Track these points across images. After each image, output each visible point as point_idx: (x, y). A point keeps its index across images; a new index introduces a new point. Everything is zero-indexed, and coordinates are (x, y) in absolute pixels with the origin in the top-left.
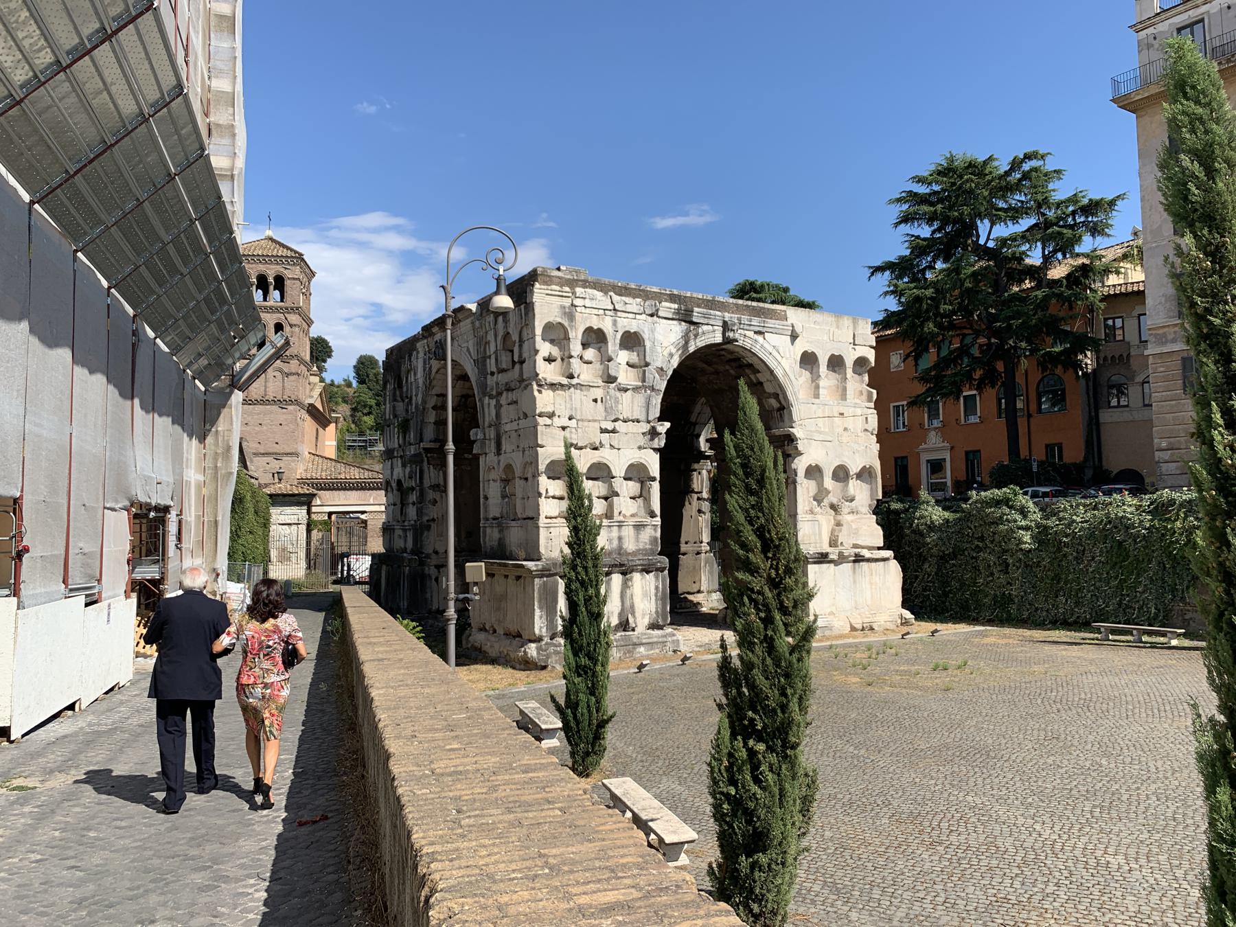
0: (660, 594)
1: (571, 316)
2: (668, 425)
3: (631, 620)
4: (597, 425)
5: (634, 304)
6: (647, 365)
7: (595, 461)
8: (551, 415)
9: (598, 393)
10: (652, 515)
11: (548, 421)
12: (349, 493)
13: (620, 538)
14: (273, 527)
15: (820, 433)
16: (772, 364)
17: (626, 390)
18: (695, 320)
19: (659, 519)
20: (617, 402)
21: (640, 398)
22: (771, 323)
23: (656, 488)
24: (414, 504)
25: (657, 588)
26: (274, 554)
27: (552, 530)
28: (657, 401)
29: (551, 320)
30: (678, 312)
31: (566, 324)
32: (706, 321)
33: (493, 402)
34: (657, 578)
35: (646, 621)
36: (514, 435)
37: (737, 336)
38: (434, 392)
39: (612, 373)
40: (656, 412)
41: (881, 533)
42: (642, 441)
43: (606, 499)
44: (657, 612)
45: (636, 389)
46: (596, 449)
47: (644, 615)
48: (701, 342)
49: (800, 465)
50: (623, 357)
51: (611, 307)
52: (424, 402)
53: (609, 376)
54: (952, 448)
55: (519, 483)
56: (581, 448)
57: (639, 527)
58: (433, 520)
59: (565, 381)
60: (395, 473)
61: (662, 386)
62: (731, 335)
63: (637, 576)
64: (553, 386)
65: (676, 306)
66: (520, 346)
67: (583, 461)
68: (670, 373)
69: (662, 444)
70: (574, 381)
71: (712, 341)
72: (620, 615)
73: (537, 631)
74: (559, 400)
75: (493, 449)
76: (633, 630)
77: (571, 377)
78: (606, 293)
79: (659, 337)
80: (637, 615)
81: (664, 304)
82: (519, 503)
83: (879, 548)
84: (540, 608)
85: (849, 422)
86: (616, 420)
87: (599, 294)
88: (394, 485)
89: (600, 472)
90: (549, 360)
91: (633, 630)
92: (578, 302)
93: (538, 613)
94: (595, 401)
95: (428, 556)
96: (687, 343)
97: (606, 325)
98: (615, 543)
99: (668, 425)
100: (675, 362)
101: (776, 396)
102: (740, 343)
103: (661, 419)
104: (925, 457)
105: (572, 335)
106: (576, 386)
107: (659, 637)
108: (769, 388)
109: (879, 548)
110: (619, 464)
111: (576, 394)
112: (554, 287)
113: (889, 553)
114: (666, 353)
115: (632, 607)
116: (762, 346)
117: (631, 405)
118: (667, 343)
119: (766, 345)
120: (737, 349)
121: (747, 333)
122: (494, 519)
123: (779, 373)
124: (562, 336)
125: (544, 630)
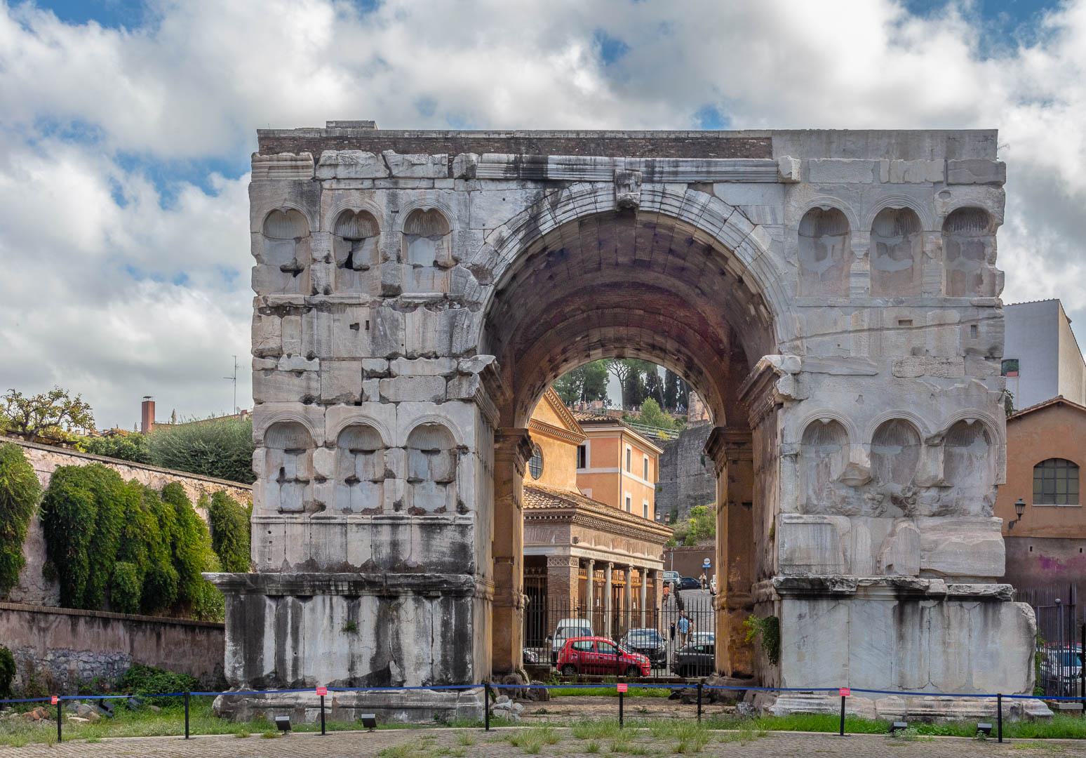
3: (394, 670)
4: (356, 365)
6: (457, 261)
7: (351, 422)
9: (362, 315)
10: (462, 509)
11: (269, 363)
13: (395, 545)
15: (844, 360)
17: (416, 306)
18: (552, 176)
20: (395, 325)
21: (438, 319)
22: (724, 164)
25: (445, 624)
27: (272, 528)
29: (278, 205)
30: (515, 166)
31: (303, 209)
32: (576, 176)
34: (446, 607)
35: (424, 674)
42: (439, 388)
45: (431, 304)
46: (358, 404)
47: (419, 665)
48: (566, 214)
51: (382, 173)
56: (329, 403)
57: (431, 528)
59: (299, 298)
61: (486, 294)
62: (622, 194)
63: (408, 605)
65: (512, 157)
68: (499, 271)
71: (591, 209)
72: (374, 661)
73: (228, 673)
74: (289, 330)
76: (400, 685)
80: (406, 664)
81: (485, 156)
83: (999, 580)
84: (234, 640)
85: (929, 340)
86: (389, 359)
87: (361, 155)
89: (359, 440)
92: (325, 173)
93: (229, 647)
94: (355, 327)
96: (535, 219)
97: (379, 203)
98: (385, 552)
100: (511, 251)
106: (321, 307)
107: (442, 700)
110: (393, 424)
112: (285, 155)
114: (491, 240)
115: (398, 649)
116: (704, 209)
119: (715, 206)
121: (670, 189)
125: (240, 673)
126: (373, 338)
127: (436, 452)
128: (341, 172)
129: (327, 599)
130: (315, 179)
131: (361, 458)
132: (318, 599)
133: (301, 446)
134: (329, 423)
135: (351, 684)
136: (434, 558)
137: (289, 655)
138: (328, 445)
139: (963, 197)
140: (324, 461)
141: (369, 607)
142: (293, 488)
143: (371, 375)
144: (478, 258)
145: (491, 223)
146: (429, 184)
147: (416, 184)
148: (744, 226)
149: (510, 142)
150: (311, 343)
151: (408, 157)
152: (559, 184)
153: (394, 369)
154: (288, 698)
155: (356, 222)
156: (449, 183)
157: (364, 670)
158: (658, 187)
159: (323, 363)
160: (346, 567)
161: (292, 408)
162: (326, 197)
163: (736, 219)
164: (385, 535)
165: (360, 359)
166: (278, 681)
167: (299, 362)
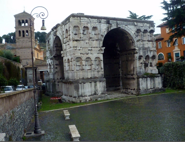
0: (104, 87)
1: (80, 24)
2: (104, 48)
3: (97, 92)
4: (87, 49)
5: (95, 20)
6: (99, 34)
7: (87, 57)
8: (76, 47)
9: (87, 41)
10: (102, 69)
11: (76, 48)
12: (44, 67)
14: (28, 75)
16: (130, 32)
18: (110, 23)
19: (103, 69)
21: (98, 42)
23: (102, 62)
24: (53, 68)
25: (103, 85)
26: (28, 81)
27: (77, 73)
28: (102, 42)
29: (75, 25)
32: (113, 23)
33: (65, 45)
34: (103, 83)
35: (101, 93)
36: (69, 52)
37: (120, 26)
38: (55, 43)
39: (91, 37)
40: (101, 45)
41: (158, 70)
42: (98, 52)
43: (91, 65)
44: (103, 91)
46: (87, 54)
47: (100, 91)
48: (112, 28)
49: (137, 56)
50: (93, 33)
52: (53, 46)
53: (90, 37)
54: (180, 50)
55: (71, 63)
57: (98, 72)
58: (57, 72)
59: (79, 39)
60: (49, 62)
61: (103, 39)
62: (119, 26)
64: (77, 41)
66: (69, 32)
67: (84, 57)
69: (103, 52)
70: (81, 39)
71: (114, 28)
72: (94, 92)
75: (66, 56)
77: (81, 38)
78: (88, 18)
79: (102, 28)
80: (98, 91)
81: (102, 20)
82: (71, 67)
86: (92, 47)
88: (49, 64)
90: (76, 34)
91: (98, 95)
92: (81, 21)
94: (87, 43)
95: (56, 80)
96: (108, 28)
99: (104, 48)
100: (106, 33)
101: (131, 40)
102: (121, 28)
103: (103, 47)
104: (174, 53)
105: (80, 28)
106: (82, 40)
108: (130, 38)
109: (157, 74)
110: (93, 57)
111: (82, 42)
112: (76, 18)
113: (159, 75)
114: (103, 31)
115: (97, 89)
116: (127, 28)
117: (95, 44)
118: (103, 29)
119: (128, 28)
120: (121, 29)
121: (123, 25)
122: (67, 71)
123: (132, 34)
124: (78, 29)
125: (77, 95)
126: (89, 45)
127: (96, 61)
128: (84, 21)
129: (88, 83)
130: (80, 22)
131: (87, 62)
132: (86, 83)
133: (79, 60)
134: (84, 57)
135: (91, 95)
136: (99, 76)
137: (83, 92)
138: (84, 60)
139: (152, 28)
140: (84, 63)
141: (93, 84)
142: (78, 67)
143: (90, 50)
144: (102, 34)
145: (103, 29)
146: (94, 23)
147: (93, 23)
148: (131, 31)
149: (104, 18)
150: (81, 45)
151: (92, 19)
152: (111, 24)
153: (92, 49)
154: (84, 98)
155: (86, 28)
156: (97, 23)
157: (93, 93)
158: (122, 25)
159: (83, 49)
160: (88, 78)
161: (79, 55)
162: (82, 24)
163: (130, 30)
164: (93, 73)
165: (88, 48)
166: (82, 96)
167: (79, 48)
